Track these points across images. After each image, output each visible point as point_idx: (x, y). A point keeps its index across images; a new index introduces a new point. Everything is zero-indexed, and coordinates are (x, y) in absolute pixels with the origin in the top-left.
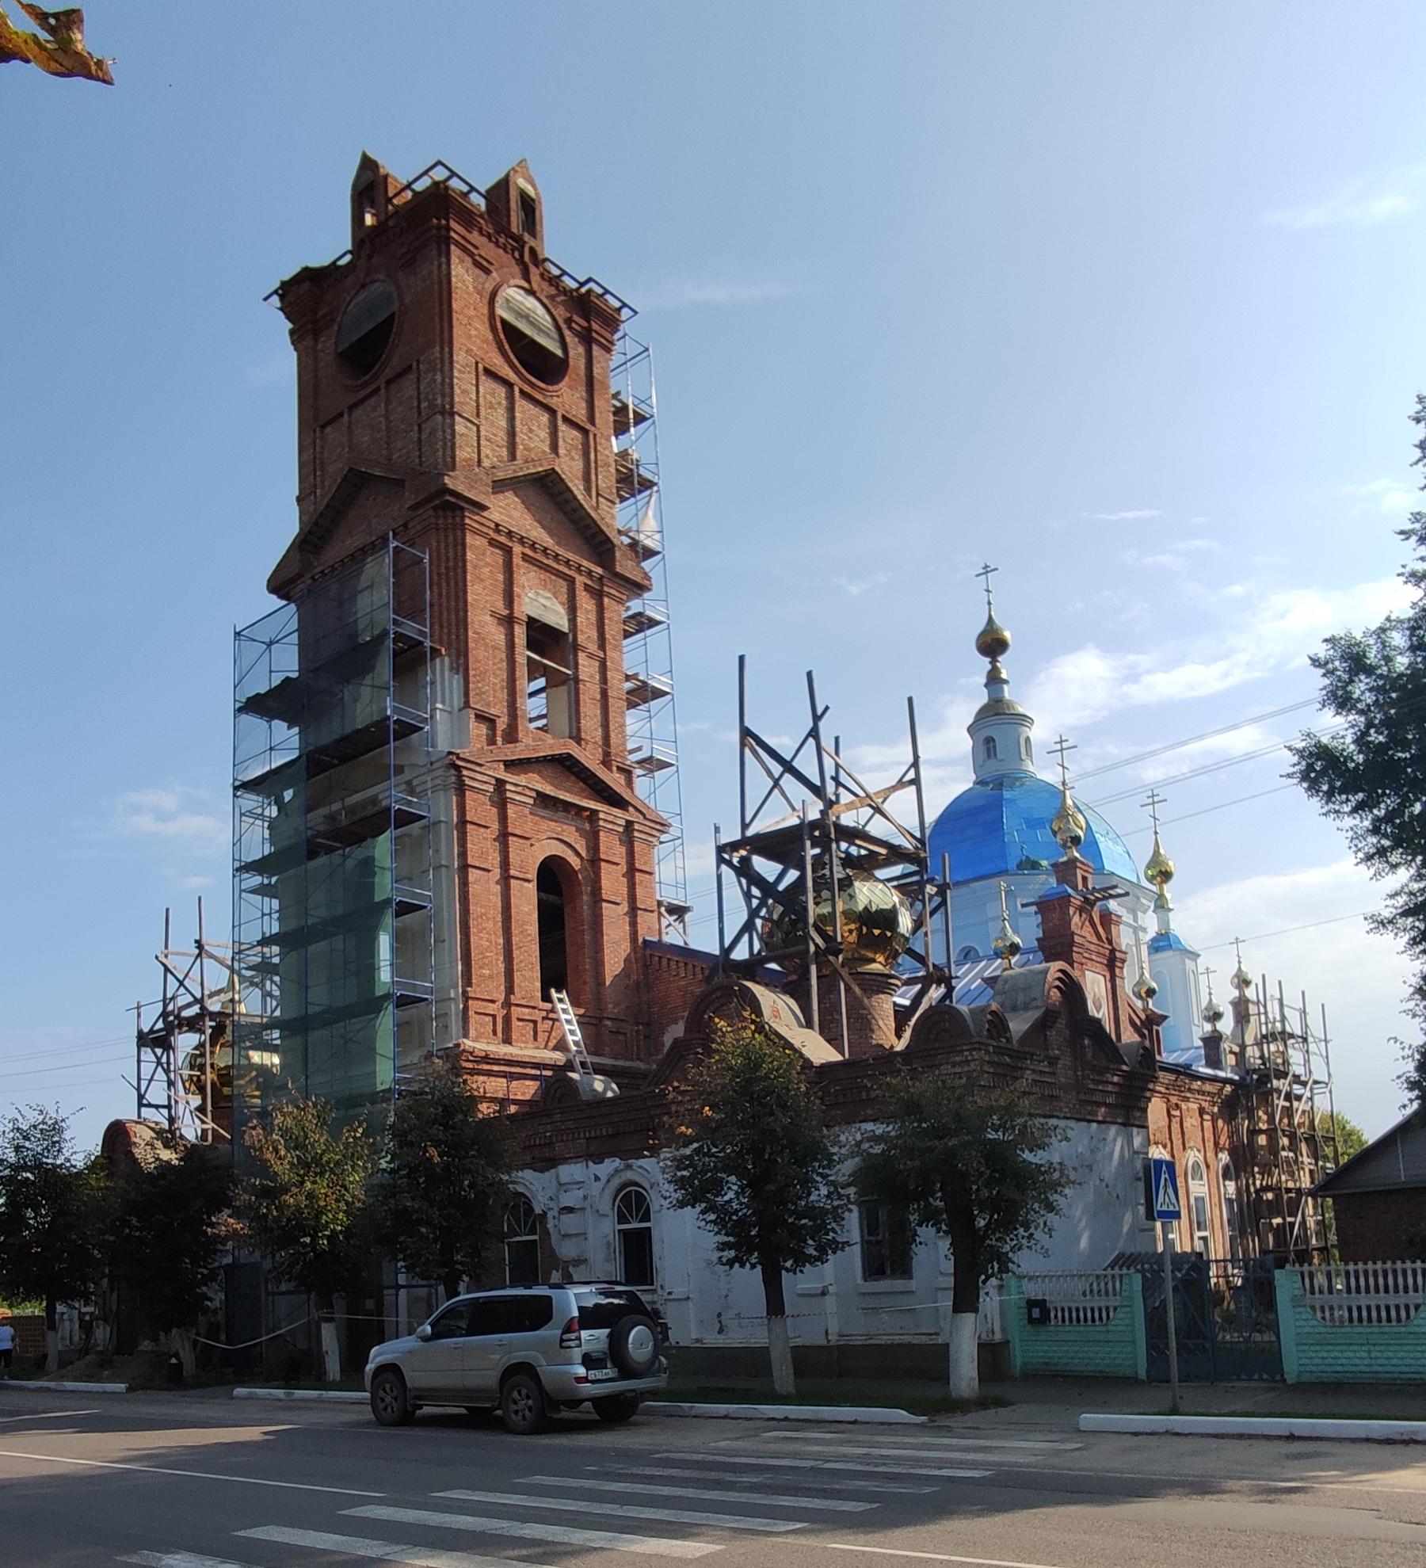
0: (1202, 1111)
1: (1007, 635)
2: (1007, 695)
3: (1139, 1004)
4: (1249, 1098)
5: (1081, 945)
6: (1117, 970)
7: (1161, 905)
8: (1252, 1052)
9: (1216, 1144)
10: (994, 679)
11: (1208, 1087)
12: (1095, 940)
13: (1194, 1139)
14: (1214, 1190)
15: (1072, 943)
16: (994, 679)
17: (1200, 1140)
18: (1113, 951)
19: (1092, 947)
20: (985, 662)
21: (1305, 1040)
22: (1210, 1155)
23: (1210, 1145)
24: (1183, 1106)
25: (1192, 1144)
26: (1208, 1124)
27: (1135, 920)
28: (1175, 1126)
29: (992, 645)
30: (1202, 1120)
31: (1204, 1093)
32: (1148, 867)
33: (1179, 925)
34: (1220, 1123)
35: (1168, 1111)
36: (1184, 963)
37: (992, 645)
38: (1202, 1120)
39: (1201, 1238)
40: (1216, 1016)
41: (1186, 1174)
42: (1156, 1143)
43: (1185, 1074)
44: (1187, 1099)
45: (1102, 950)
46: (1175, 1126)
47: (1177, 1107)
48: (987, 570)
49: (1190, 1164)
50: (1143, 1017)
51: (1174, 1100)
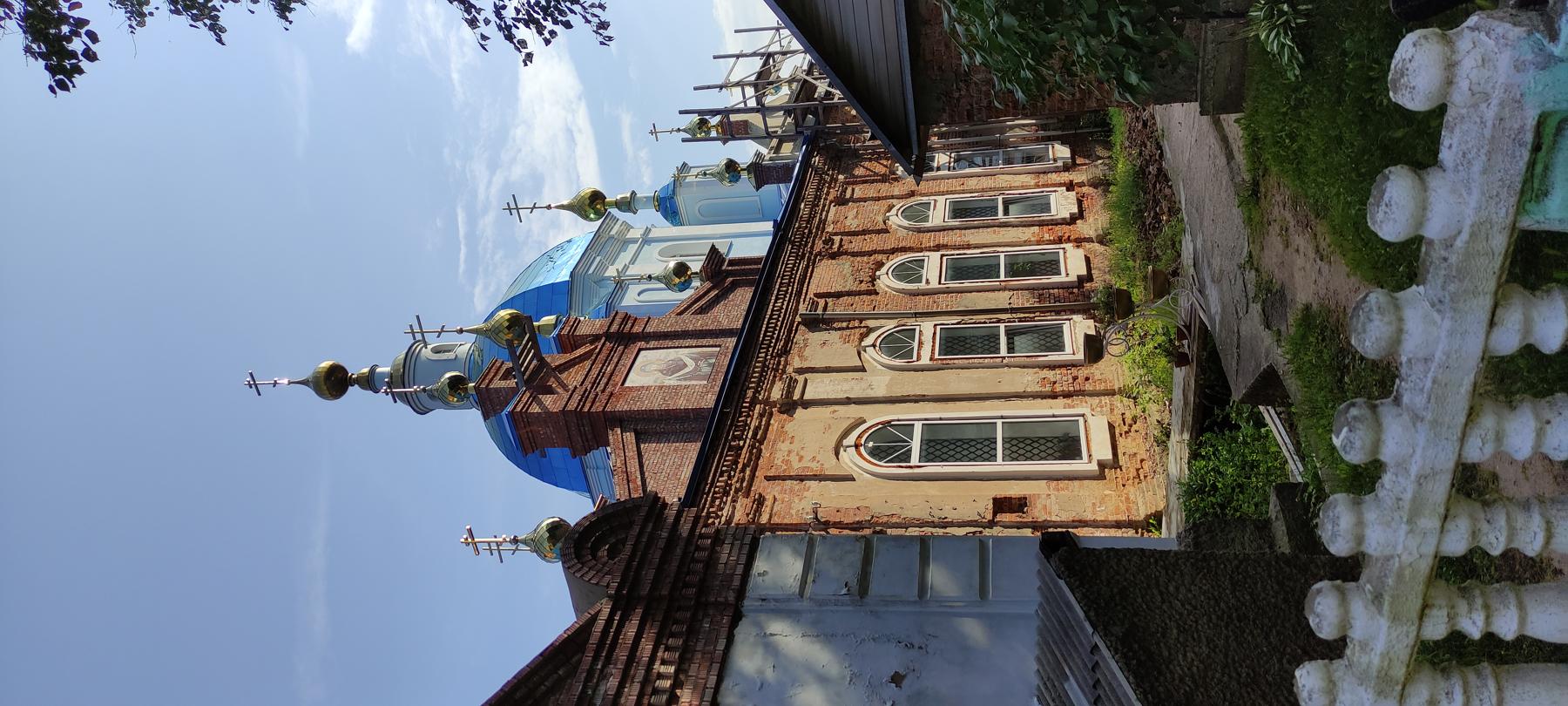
0: (841, 201)
1: (326, 364)
2: (387, 369)
3: (696, 283)
4: (832, 132)
5: (584, 398)
6: (637, 329)
7: (628, 205)
8: (776, 122)
9: (884, 179)
10: (369, 382)
11: (810, 192)
12: (588, 363)
13: (870, 214)
14: (944, 186)
15: (578, 413)
16: (369, 382)
17: (876, 206)
18: (608, 336)
19: (595, 372)
20: (354, 391)
21: (770, 55)
22: (897, 189)
23: (884, 189)
24: (830, 229)
25: (880, 219)
26: (859, 191)
27: (634, 241)
28: (856, 244)
29: (334, 382)
30: (852, 199)
31: (818, 198)
32: (586, 217)
33: (649, 184)
34: (859, 171)
35: (833, 256)
36: (690, 184)
37: (334, 382)
38: (852, 199)
39: (1006, 212)
40: (731, 166)
41: (919, 231)
42: (873, 279)
43: (786, 230)
44: (823, 222)
45: (605, 352)
46: (856, 244)
47: (829, 241)
48: (253, 384)
49: (906, 223)
50: (708, 285)
51: (819, 245)
